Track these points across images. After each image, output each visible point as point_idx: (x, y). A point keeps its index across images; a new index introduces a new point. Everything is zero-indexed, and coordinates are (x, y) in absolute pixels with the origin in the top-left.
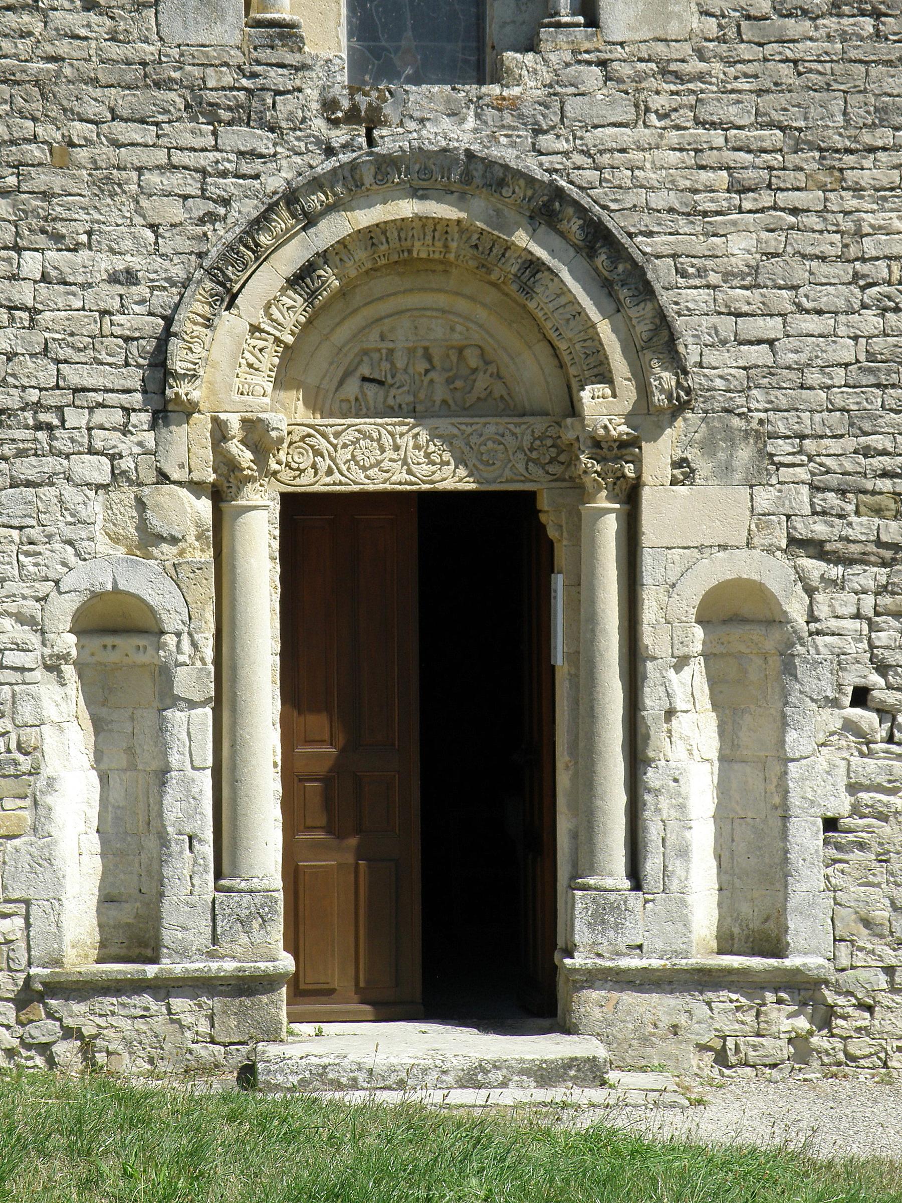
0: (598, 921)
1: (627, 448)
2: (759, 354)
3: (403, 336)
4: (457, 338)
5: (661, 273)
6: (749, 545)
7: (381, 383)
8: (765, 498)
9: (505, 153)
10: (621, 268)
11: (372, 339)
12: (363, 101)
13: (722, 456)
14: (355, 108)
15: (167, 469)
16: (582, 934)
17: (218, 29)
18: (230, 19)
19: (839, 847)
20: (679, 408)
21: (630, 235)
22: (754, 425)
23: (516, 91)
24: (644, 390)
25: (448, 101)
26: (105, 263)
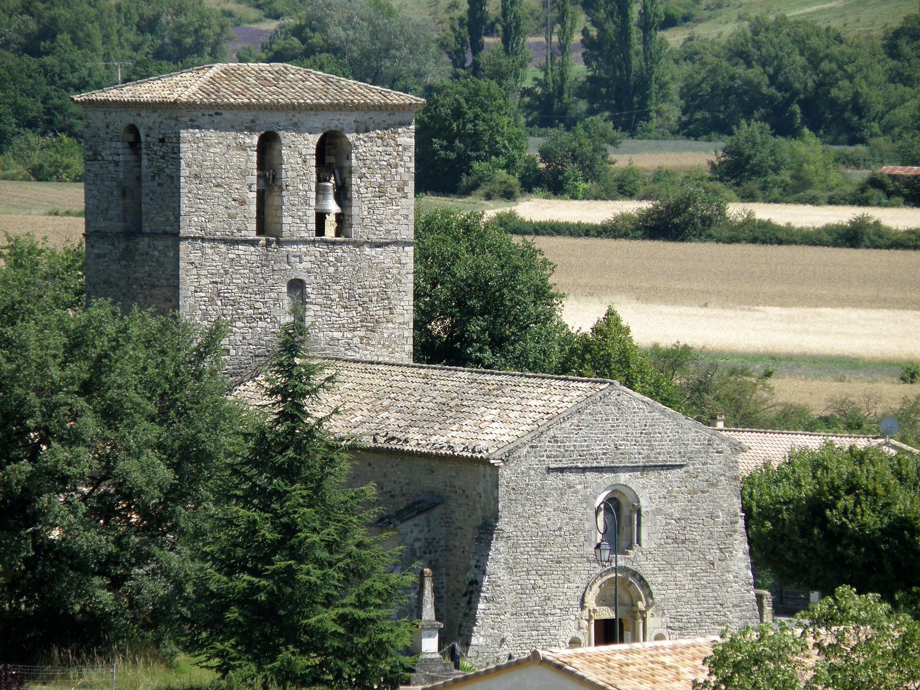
1: (645, 612)
5: (650, 584)
8: (663, 620)
9: (628, 566)
20: (652, 605)
24: (647, 602)
26: (575, 585)
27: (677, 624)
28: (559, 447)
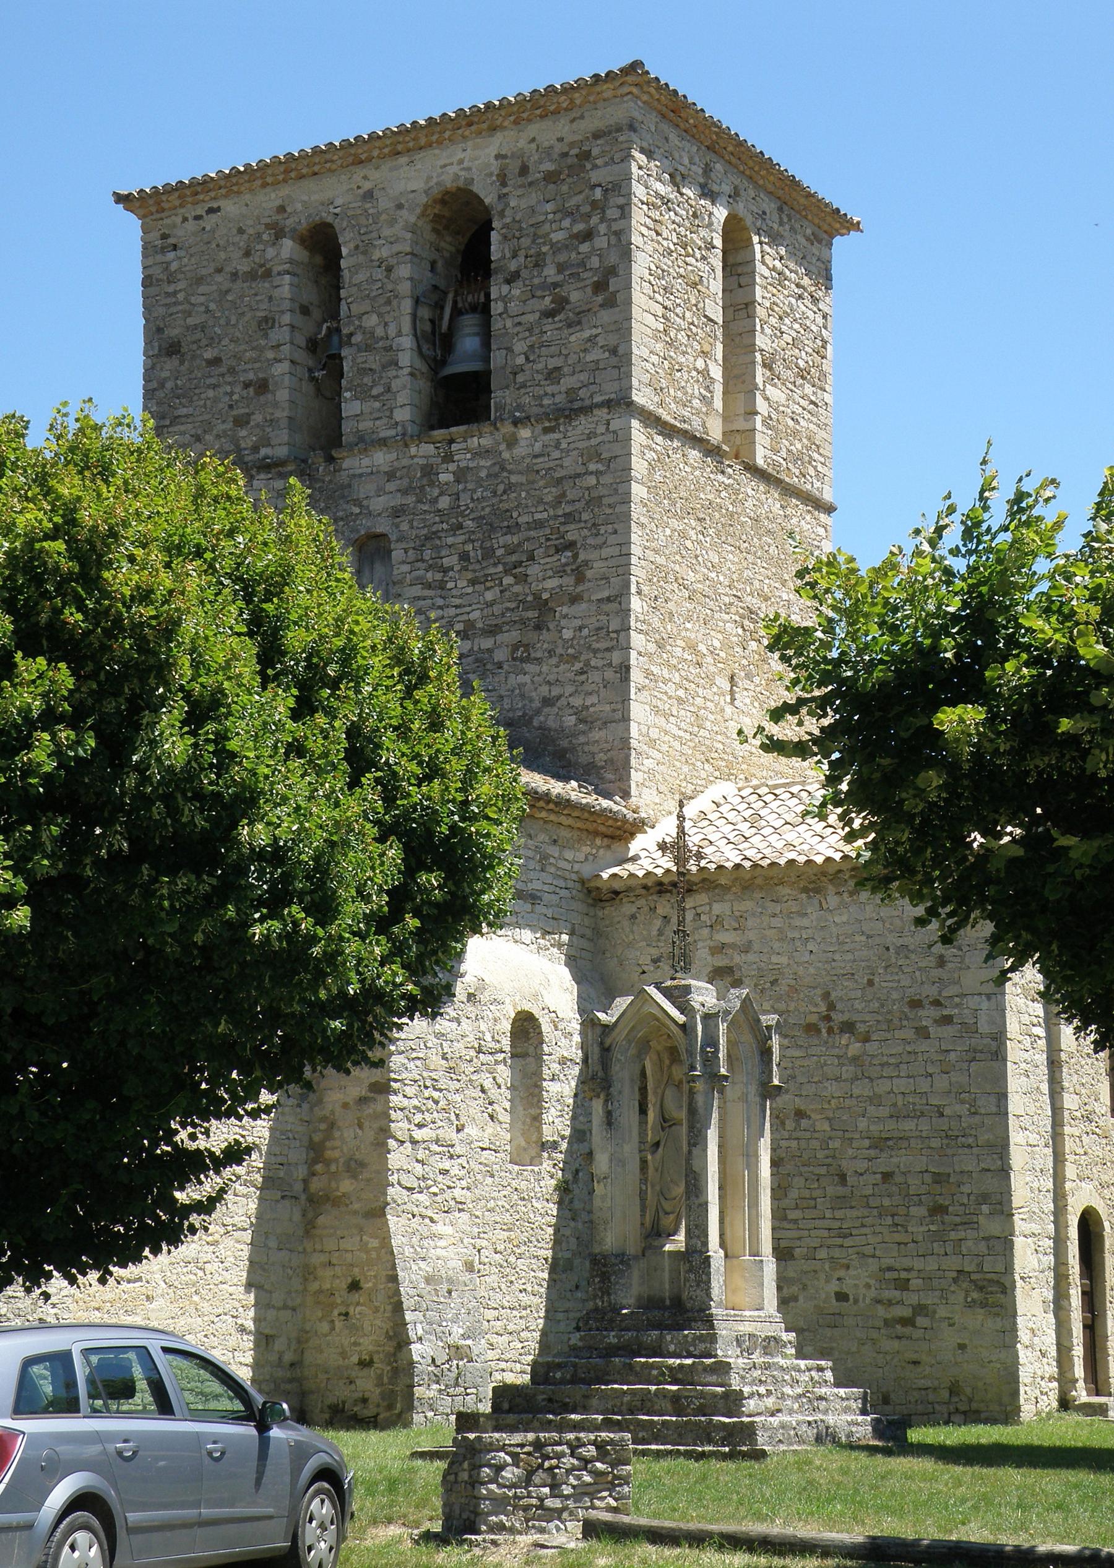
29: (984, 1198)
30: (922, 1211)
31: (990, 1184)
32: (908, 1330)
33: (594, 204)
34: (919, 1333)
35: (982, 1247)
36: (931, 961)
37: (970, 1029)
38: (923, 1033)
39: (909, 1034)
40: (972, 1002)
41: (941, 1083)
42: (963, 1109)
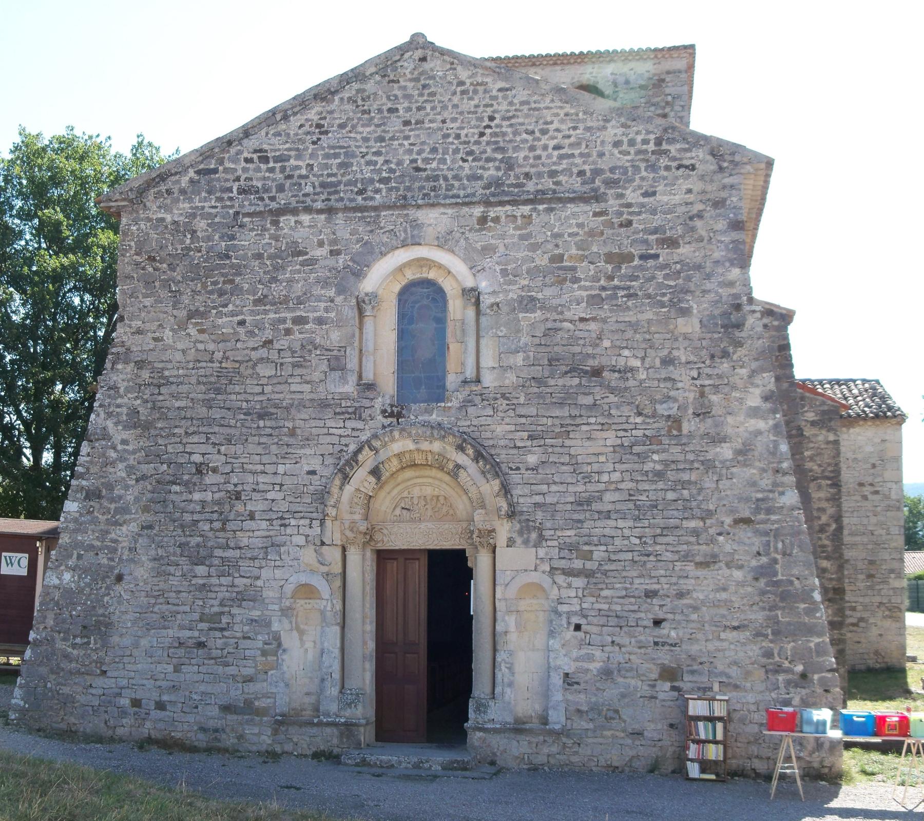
0: (478, 710)
2: (539, 499)
3: (416, 492)
4: (436, 493)
6: (535, 570)
7: (408, 510)
8: (542, 552)
10: (488, 467)
11: (405, 494)
12: (395, 410)
13: (525, 536)
14: (392, 412)
15: (324, 540)
16: (471, 714)
17: (346, 386)
18: (350, 383)
19: (569, 684)
21: (492, 455)
22: (537, 524)
23: (449, 405)
25: (426, 409)
27: (578, 564)
28: (271, 170)
29: (892, 571)
30: (861, 577)
31: (895, 565)
32: (855, 628)
33: (667, 103)
34: (860, 630)
35: (891, 592)
36: (869, 466)
37: (887, 497)
38: (865, 498)
39: (859, 498)
40: (889, 485)
41: (874, 520)
42: (883, 532)
